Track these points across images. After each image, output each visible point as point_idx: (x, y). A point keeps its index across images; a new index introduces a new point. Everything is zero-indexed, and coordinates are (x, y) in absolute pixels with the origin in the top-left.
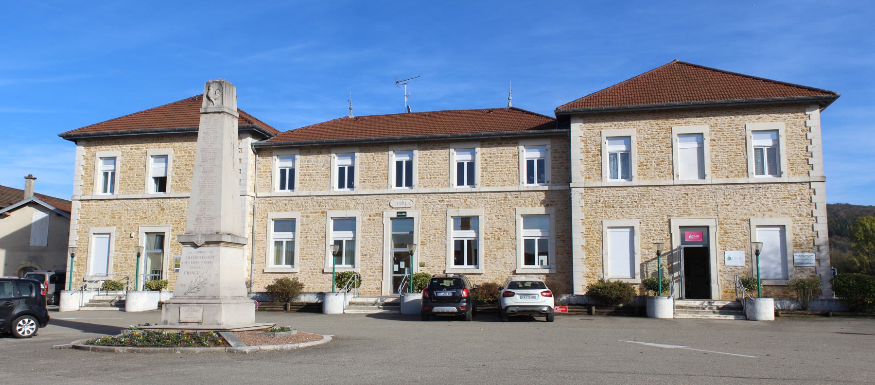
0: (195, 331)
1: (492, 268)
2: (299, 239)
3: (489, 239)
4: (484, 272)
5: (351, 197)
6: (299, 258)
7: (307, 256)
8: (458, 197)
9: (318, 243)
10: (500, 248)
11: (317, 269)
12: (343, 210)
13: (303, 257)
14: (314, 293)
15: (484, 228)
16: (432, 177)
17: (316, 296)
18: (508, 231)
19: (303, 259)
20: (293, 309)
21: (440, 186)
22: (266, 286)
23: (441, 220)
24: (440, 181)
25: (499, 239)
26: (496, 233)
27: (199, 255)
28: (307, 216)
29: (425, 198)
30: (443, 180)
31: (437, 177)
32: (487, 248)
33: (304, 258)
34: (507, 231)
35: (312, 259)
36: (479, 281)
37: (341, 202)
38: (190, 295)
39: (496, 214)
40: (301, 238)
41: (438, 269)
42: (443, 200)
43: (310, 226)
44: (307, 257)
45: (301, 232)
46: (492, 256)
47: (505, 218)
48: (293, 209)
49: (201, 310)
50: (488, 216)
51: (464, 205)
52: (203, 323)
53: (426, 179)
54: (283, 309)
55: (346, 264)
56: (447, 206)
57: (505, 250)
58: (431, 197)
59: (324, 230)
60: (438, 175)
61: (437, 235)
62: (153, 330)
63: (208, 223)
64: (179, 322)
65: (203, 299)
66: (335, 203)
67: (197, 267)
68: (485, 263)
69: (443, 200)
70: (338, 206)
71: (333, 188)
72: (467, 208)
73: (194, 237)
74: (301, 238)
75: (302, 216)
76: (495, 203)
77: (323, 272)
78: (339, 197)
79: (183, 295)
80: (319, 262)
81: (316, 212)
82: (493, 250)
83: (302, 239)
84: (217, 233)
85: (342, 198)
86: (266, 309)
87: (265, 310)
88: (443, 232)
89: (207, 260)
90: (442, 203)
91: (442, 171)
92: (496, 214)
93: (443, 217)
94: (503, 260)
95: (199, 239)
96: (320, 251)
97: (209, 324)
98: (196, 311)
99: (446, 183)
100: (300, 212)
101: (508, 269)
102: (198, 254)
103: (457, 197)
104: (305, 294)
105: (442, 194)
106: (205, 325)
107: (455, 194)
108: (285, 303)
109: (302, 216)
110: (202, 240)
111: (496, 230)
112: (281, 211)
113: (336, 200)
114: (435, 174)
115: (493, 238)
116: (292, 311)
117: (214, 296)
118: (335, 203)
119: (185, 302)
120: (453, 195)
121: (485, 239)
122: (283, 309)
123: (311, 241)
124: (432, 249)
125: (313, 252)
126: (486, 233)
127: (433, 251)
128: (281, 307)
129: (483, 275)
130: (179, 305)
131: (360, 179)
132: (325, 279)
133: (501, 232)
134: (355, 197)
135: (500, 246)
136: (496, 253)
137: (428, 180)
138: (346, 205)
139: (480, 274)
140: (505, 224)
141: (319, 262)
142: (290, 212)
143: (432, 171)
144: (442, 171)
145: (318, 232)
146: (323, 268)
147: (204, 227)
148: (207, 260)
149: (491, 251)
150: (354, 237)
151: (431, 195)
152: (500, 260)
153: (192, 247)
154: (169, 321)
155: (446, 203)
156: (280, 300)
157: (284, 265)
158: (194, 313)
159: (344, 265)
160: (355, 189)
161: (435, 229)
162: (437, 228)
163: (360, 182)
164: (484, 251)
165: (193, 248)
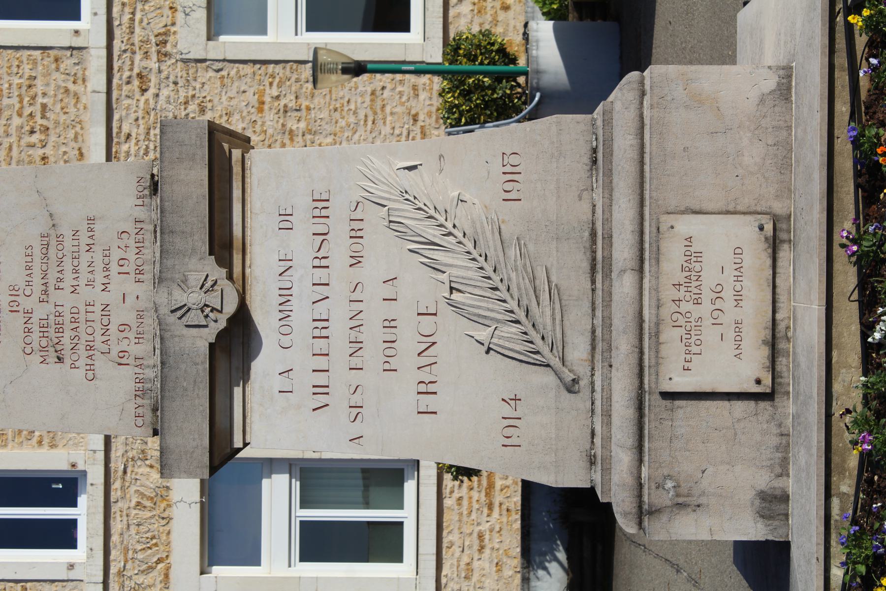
0: (840, 255)
5: (116, 485)
8: (127, 10)
12: (169, 519)
14: (526, 580)
16: (40, 121)
17: (541, 573)
21: (79, 88)
23: (223, 86)
24: (59, 87)
29: (128, 154)
30: (56, 75)
31: (40, 100)
37: (133, 530)
41: (423, 96)
42: (140, 76)
49: (686, 225)
52: (779, 208)
53: (48, 151)
55: (400, 506)
56: (163, 56)
58: (126, 129)
60: (34, 98)
61: (283, 102)
62: (839, 554)
63: (85, 258)
64: (768, 397)
65: (609, 238)
66: (140, 556)
67: (390, 324)
69: (140, 76)
70: (151, 543)
71: (71, 566)
73: (174, 346)
78: (115, 538)
79: (581, 402)
84: (155, 187)
85: (117, 526)
88: (273, 76)
90: (153, 79)
91: (16, 81)
93: (211, 73)
95: (195, 298)
98: (692, 257)
99: (68, 63)
103: (127, 17)
105: (115, 81)
106: (786, 191)
107: (116, 23)
110: (195, 279)
113: (126, 550)
114: (27, 111)
117: (586, 159)
118: (140, 556)
119: (633, 360)
120: (117, 32)
124: (342, 123)
127: (352, 119)
130: (654, 404)
131: (40, 443)
134: (117, 465)
137: (53, 138)
138: (148, 504)
143: (16, 121)
144: (16, 81)
147: (112, 297)
150: (289, 465)
151: (115, 125)
153: (245, 375)
154: (763, 480)
155: (153, 64)
158: (710, 279)
159: (406, 515)
160: (81, 467)
161: (260, 110)
162: (254, 100)
163: (53, 446)
165: (258, 366)
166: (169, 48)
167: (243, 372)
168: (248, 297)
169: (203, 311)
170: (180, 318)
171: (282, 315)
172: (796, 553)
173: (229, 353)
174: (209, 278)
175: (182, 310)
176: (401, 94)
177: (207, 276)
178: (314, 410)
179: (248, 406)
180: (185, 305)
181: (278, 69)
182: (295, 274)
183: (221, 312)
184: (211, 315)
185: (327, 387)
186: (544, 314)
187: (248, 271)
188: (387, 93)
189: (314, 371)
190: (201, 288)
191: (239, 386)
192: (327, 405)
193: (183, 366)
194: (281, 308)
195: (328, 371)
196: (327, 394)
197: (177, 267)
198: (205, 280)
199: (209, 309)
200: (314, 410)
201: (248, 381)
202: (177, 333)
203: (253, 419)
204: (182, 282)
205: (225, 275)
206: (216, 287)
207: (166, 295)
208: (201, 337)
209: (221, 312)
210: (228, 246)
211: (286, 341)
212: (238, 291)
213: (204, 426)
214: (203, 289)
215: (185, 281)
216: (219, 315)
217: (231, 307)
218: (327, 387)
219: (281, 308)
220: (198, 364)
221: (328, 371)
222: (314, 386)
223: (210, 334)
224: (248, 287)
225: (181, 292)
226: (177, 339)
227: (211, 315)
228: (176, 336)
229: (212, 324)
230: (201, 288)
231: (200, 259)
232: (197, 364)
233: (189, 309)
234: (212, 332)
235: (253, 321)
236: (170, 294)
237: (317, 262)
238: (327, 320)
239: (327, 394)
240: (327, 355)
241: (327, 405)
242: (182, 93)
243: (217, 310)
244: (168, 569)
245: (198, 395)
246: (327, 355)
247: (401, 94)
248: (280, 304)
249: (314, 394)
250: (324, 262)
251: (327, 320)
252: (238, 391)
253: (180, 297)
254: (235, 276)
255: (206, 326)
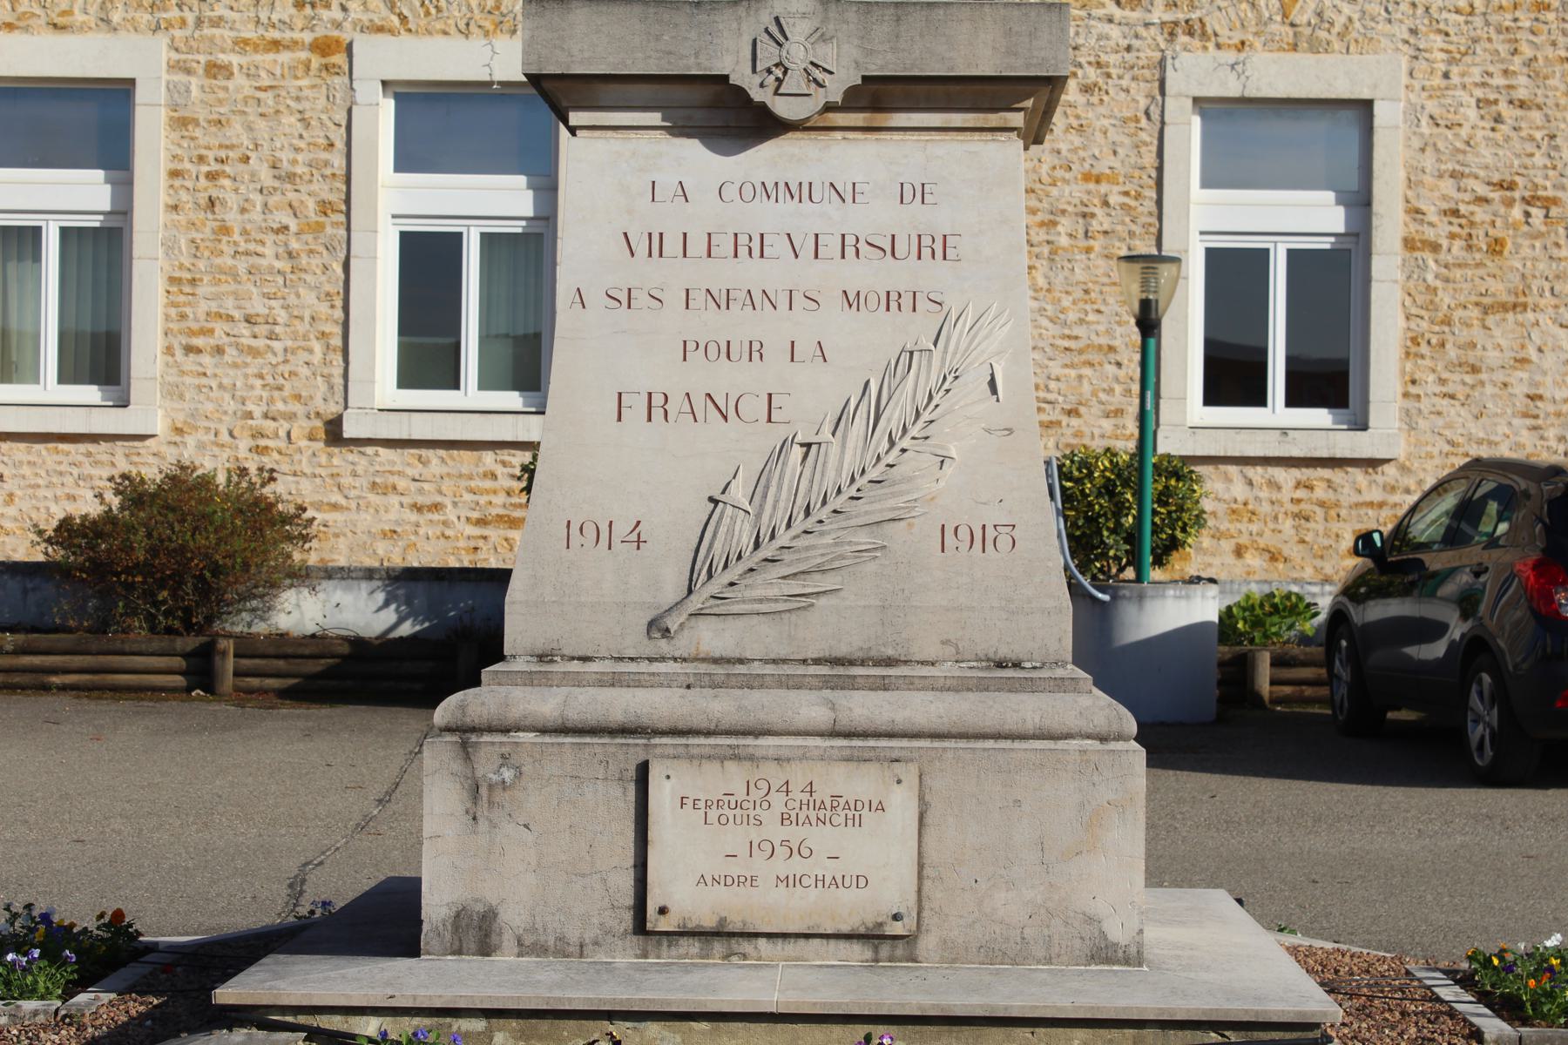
1: (1449, 426)
2: (162, 217)
3: (1435, 247)
4: (1399, 450)
6: (159, 343)
7: (220, 327)
9: (295, 245)
10: (1504, 307)
11: (291, 417)
13: (192, 333)
14: (369, 574)
15: (1402, 174)
17: (380, 597)
18: (1555, 201)
19: (189, 349)
20: (255, 682)
22: (50, 527)
23: (1125, 121)
25: (1496, 249)
26: (1481, 214)
27: (772, 217)
28: (215, 70)
32: (1422, 301)
33: (199, 342)
34: (1548, 203)
35: (254, 352)
36: (1371, 504)
38: (711, 638)
39: (1479, 93)
40: (175, 208)
41: (1107, 425)
43: (236, 132)
44: (219, 337)
45: (175, 174)
46: (1452, 352)
47: (1536, 116)
48: (116, 17)
49: (902, 804)
50: (1432, 107)
51: (1278, 28)
52: (928, 944)
54: (179, 680)
55: (484, 385)
57: (1530, 316)
59: (338, 161)
61: (1099, 211)
64: (640, 925)
65: (884, 685)
67: (755, 351)
68: (1406, 395)
72: (1295, 47)
74: (175, 208)
75: (174, 67)
76: (1478, 21)
77: (334, 433)
79: (634, 640)
80: (304, 371)
81: (276, 45)
82: (1458, 314)
83: (181, 218)
86: (56, 680)
87: (45, 688)
88: (1138, 196)
89: (869, 274)
92: (1479, 93)
94: (1520, 382)
95: (797, 53)
96: (309, 297)
97: (996, 954)
98: (853, 812)
100: (162, 40)
101: (1551, 433)
102: (762, 206)
104: (303, 576)
106: (953, 956)
108: (191, 642)
109: (174, 67)
110: (827, 54)
111: (1482, 190)
112: (26, 29)
115: (1458, 245)
116: (250, 691)
117: (1004, 652)
119: (698, 721)
121: (1409, 244)
122: (179, 680)
123: (245, 232)
124: (1066, 302)
125: (258, 306)
126: (1415, 212)
127: (1072, 316)
128: (164, 667)
129: (1390, 470)
130: (631, 752)
132: (346, 481)
133: (1509, 203)
135: (1499, 289)
136: (1477, 333)
139: (1372, 464)
140: (1539, 160)
141: (304, 371)
142: (90, 35)
145: (291, 177)
146: (332, 409)
148: (869, 274)
149: (1447, 321)
150: (546, 216)
152: (1500, 376)
153: (679, 129)
154: (513, 917)
156: (151, 618)
157: (49, 387)
158: (820, 837)
159: (470, 393)
161: (1087, 177)
162: (1102, 167)
164: (1401, 322)
165: (693, 150)
166: (1183, 39)
167: (683, 127)
168: (798, 135)
169: (777, 65)
170: (766, 30)
171: (770, 187)
172: (141, 95)
173: (713, 105)
174: (828, 75)
175: (779, 33)
176: (1110, 391)
177: (831, 73)
178: (625, 234)
179: (632, 134)
180: (787, 39)
181: (1150, 205)
182: (833, 207)
183: (776, 93)
184: (772, 77)
185: (661, 255)
186: (769, 585)
187: (838, 135)
188: (1111, 369)
189: (685, 234)
190: (812, 63)
191: (663, 120)
192: (633, 255)
193: (693, 35)
194: (782, 186)
195: (685, 256)
196: (650, 255)
197: (845, 26)
198: (825, 70)
199: (781, 76)
200: (625, 234)
201: (674, 135)
202: (744, 27)
203: (612, 141)
204: (822, 35)
205: (831, 99)
206: (813, 85)
207: (802, 10)
208: (738, 62)
209: (776, 93)
210: (877, 106)
211: (731, 192)
212: (808, 119)
213: (603, 67)
214: (810, 67)
215: (824, 39)
216: (771, 90)
217: (784, 108)
218: (661, 255)
219: (782, 186)
220: (697, 57)
221: (685, 256)
222: (661, 234)
223: (742, 76)
224: (813, 135)
225: (808, 32)
226: (735, 25)
227: (772, 77)
228: (739, 24)
229: (757, 80)
230: (812, 63)
231: (856, 63)
232: (697, 55)
233: (780, 45)
234: (747, 80)
235: (761, 142)
236: (804, 16)
237: (850, 240)
238: (762, 256)
239: (650, 255)
240: (709, 256)
241: (633, 255)
242: (1113, 59)
243: (778, 88)
244: (391, 31)
245: (650, 57)
246: (709, 256)
247: (1110, 391)
248: (787, 184)
249: (650, 234)
250: (850, 251)
251: (762, 256)
252: (655, 118)
253: (798, 31)
254: (830, 115)
255: (754, 71)
